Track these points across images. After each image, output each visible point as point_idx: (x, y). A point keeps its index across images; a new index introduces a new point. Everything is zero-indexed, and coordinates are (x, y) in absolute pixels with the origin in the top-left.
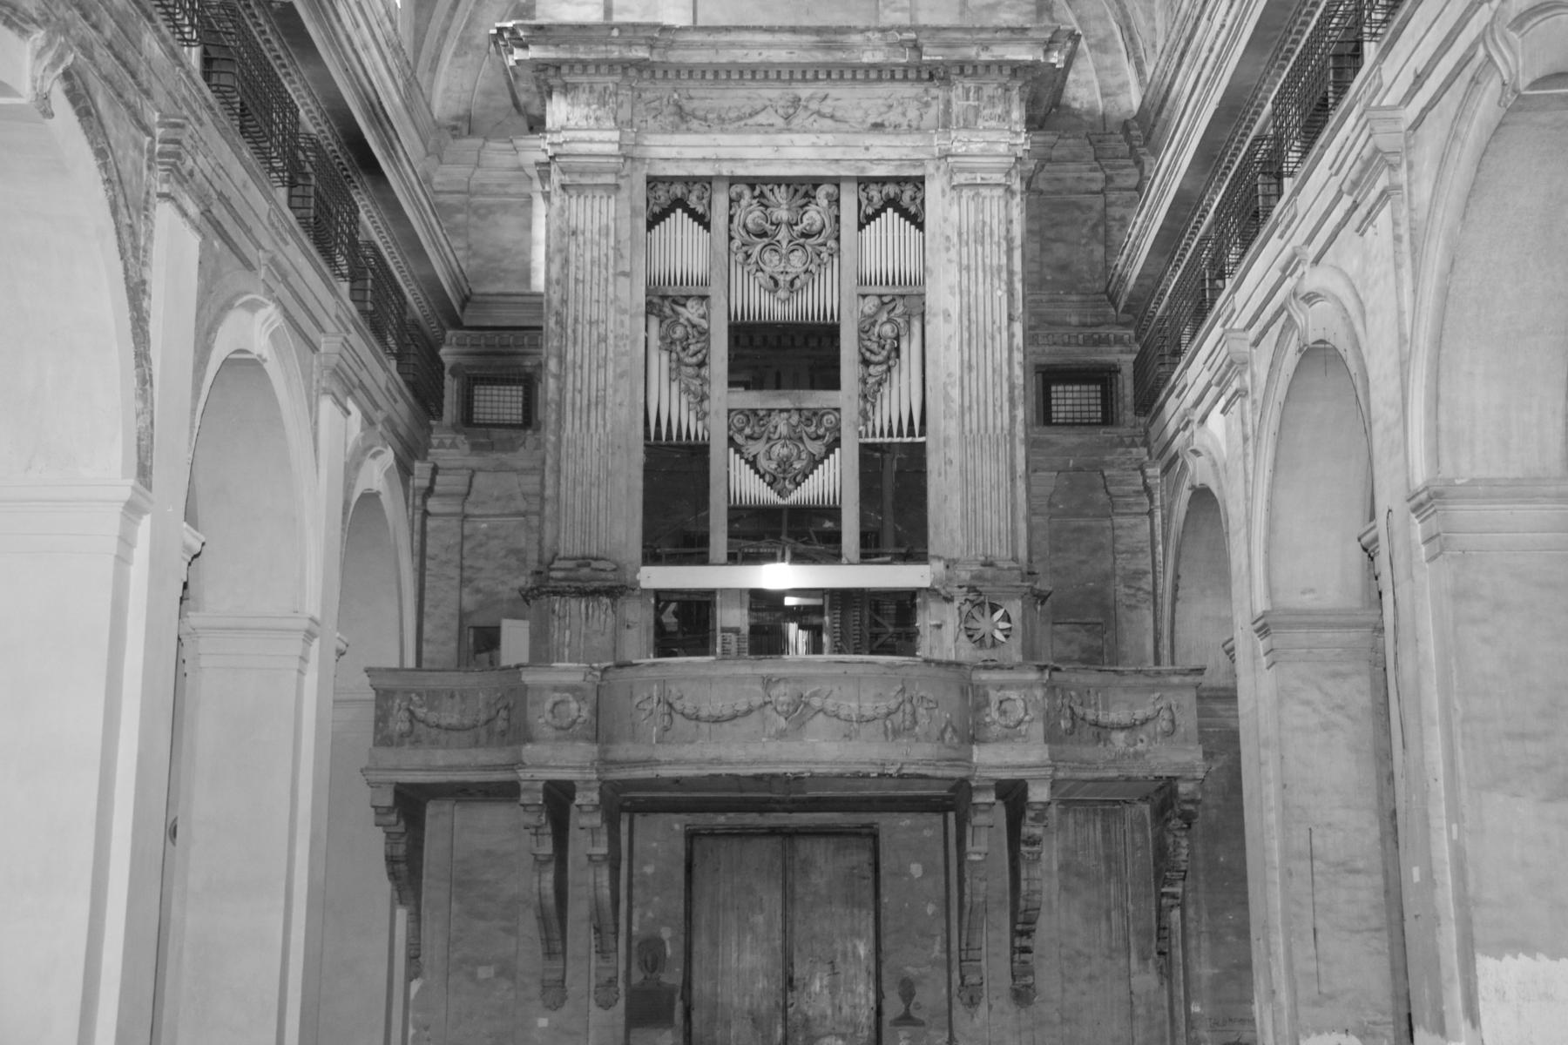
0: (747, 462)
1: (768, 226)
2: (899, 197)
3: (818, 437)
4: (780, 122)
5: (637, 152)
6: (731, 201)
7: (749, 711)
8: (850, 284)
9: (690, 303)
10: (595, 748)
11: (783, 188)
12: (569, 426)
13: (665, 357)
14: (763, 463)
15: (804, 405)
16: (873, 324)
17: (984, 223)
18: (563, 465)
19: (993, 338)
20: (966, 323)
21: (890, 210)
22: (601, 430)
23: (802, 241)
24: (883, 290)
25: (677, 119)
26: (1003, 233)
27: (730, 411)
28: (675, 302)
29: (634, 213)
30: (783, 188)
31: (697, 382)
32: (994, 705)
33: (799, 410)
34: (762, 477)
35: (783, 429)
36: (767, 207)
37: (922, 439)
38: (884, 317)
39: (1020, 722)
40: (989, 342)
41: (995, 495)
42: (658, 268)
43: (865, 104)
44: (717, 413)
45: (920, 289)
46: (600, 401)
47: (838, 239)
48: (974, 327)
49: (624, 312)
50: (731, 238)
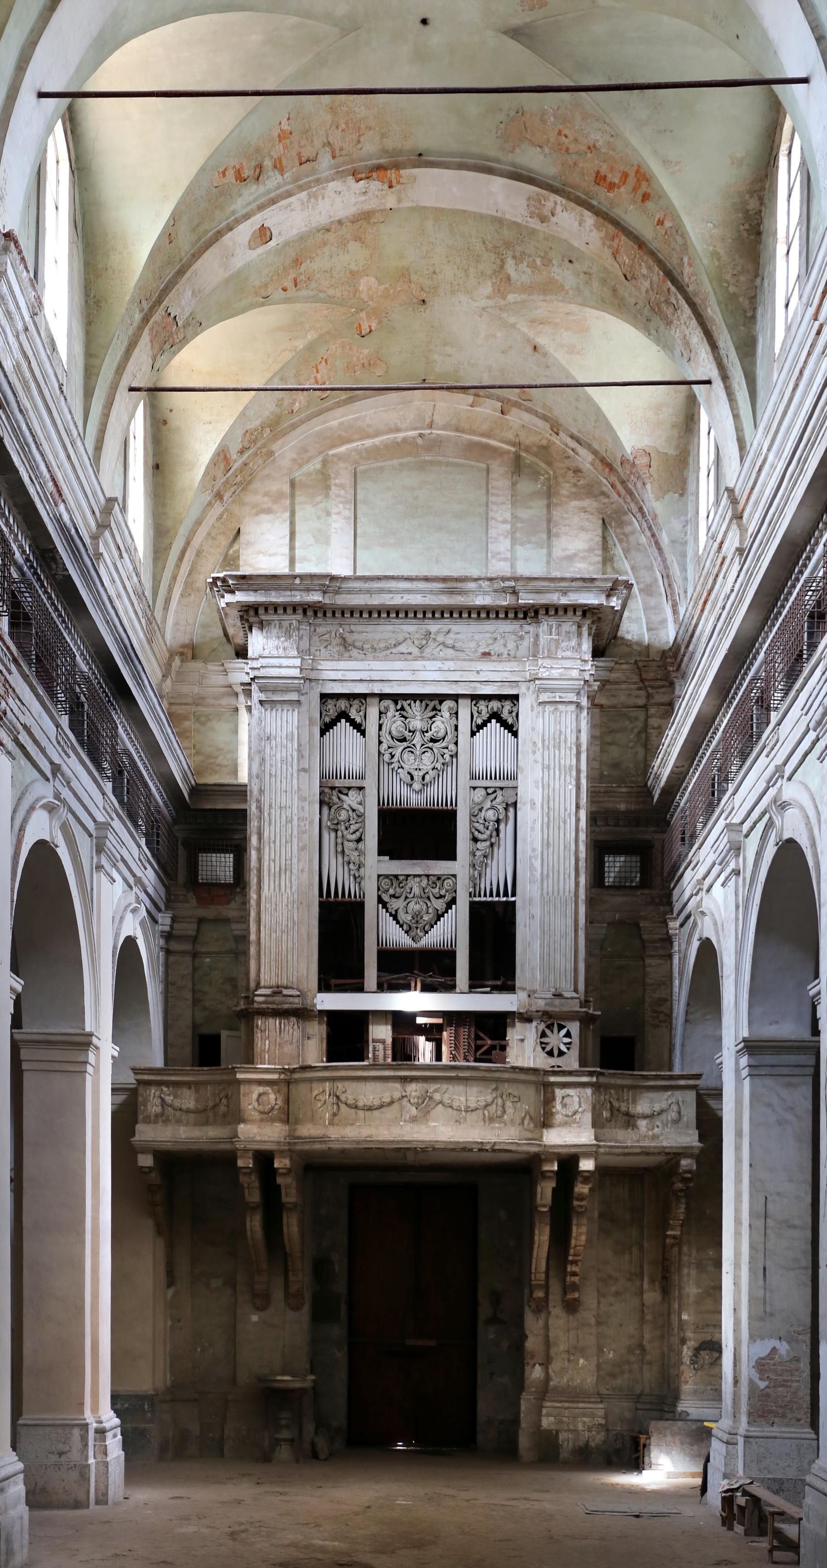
1: (407, 734)
2: (499, 711)
5: (313, 675)
6: (381, 713)
8: (464, 780)
9: (351, 793)
11: (418, 702)
13: (333, 835)
15: (431, 873)
16: (480, 810)
18: (263, 916)
22: (288, 890)
23: (430, 744)
28: (340, 792)
29: (311, 722)
30: (418, 702)
31: (356, 853)
33: (428, 876)
36: (406, 718)
38: (488, 805)
44: (370, 878)
47: (456, 743)
50: (380, 742)
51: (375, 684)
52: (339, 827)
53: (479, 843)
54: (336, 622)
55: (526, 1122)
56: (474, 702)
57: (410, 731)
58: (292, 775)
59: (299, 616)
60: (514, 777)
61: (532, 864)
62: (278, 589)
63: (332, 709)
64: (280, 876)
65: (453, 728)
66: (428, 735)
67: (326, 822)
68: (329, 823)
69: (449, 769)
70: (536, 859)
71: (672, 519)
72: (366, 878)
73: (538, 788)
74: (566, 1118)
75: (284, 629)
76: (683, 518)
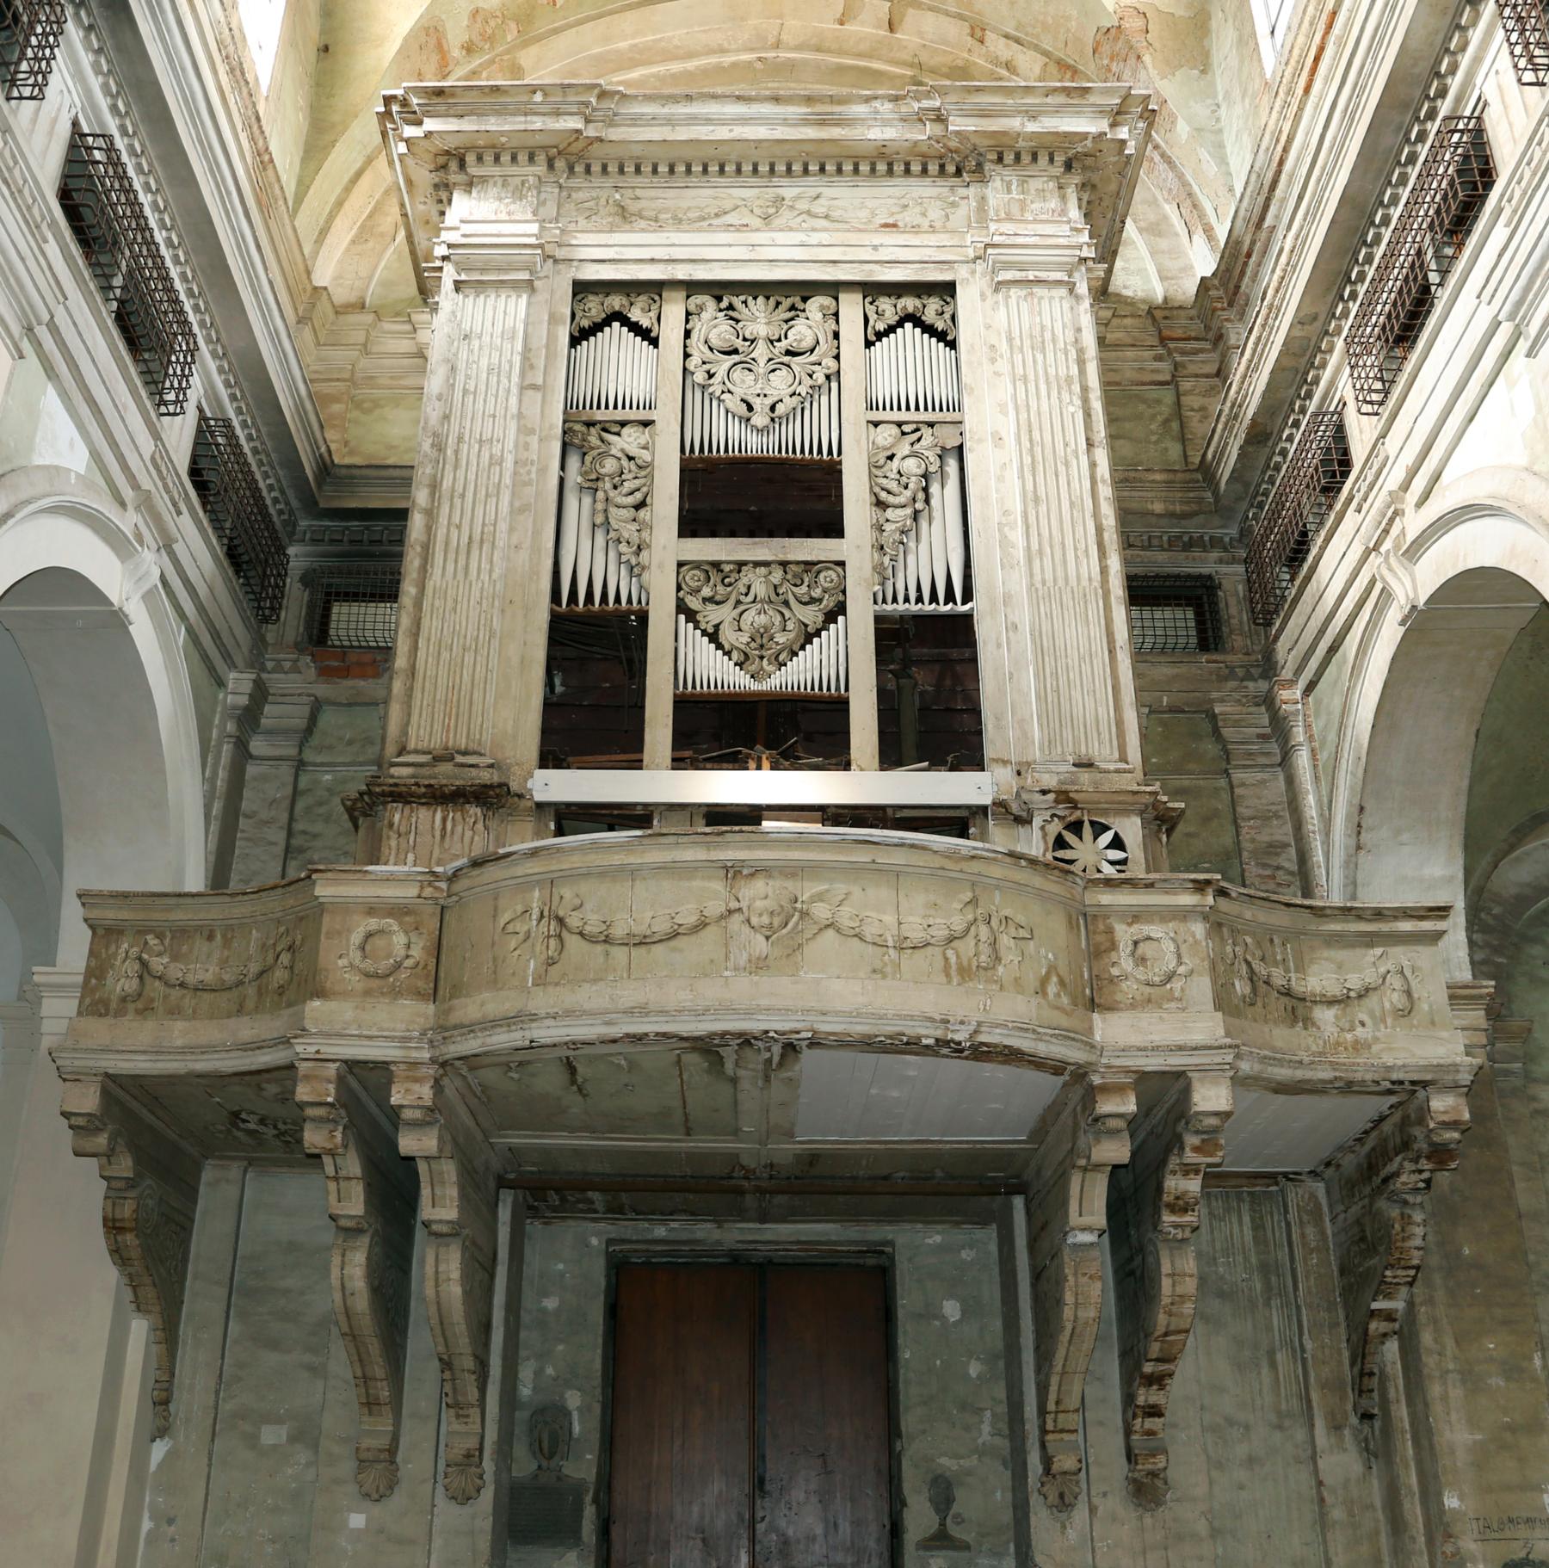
0: (704, 633)
1: (739, 343)
2: (923, 306)
3: (813, 601)
4: (757, 222)
5: (560, 253)
6: (688, 314)
7: (702, 925)
8: (854, 411)
9: (626, 431)
10: (431, 1008)
11: (761, 299)
12: (437, 571)
14: (728, 636)
15: (791, 557)
16: (891, 458)
17: (1043, 327)
18: (425, 622)
19: (1067, 464)
20: (1026, 444)
21: (908, 325)
22: (485, 577)
23: (786, 359)
24: (903, 416)
25: (618, 219)
26: (1070, 337)
27: (680, 565)
28: (605, 430)
29: (553, 319)
30: (761, 299)
31: (635, 526)
32: (1124, 947)
33: (784, 564)
34: (728, 653)
35: (760, 589)
36: (737, 321)
37: (962, 609)
38: (905, 449)
39: (1170, 977)
40: (1062, 469)
41: (1086, 669)
42: (583, 389)
43: (870, 204)
44: (661, 566)
45: (955, 416)
46: (485, 540)
47: (837, 357)
48: (1038, 450)
49: (532, 432)
50: (687, 356)
51: (679, 266)
52: (600, 484)
53: (889, 510)
54: (608, 182)
55: (1052, 989)
56: (869, 299)
57: (745, 339)
58: (509, 391)
59: (540, 168)
60: (957, 407)
61: (1003, 538)
62: (501, 112)
63: (595, 308)
64: (468, 552)
65: (830, 336)
66: (784, 344)
67: (574, 475)
68: (579, 479)
69: (824, 399)
70: (1013, 527)
71: (1192, 103)
72: (653, 568)
73: (1006, 414)
74: (1148, 990)
75: (510, 189)
76: (1209, 101)
